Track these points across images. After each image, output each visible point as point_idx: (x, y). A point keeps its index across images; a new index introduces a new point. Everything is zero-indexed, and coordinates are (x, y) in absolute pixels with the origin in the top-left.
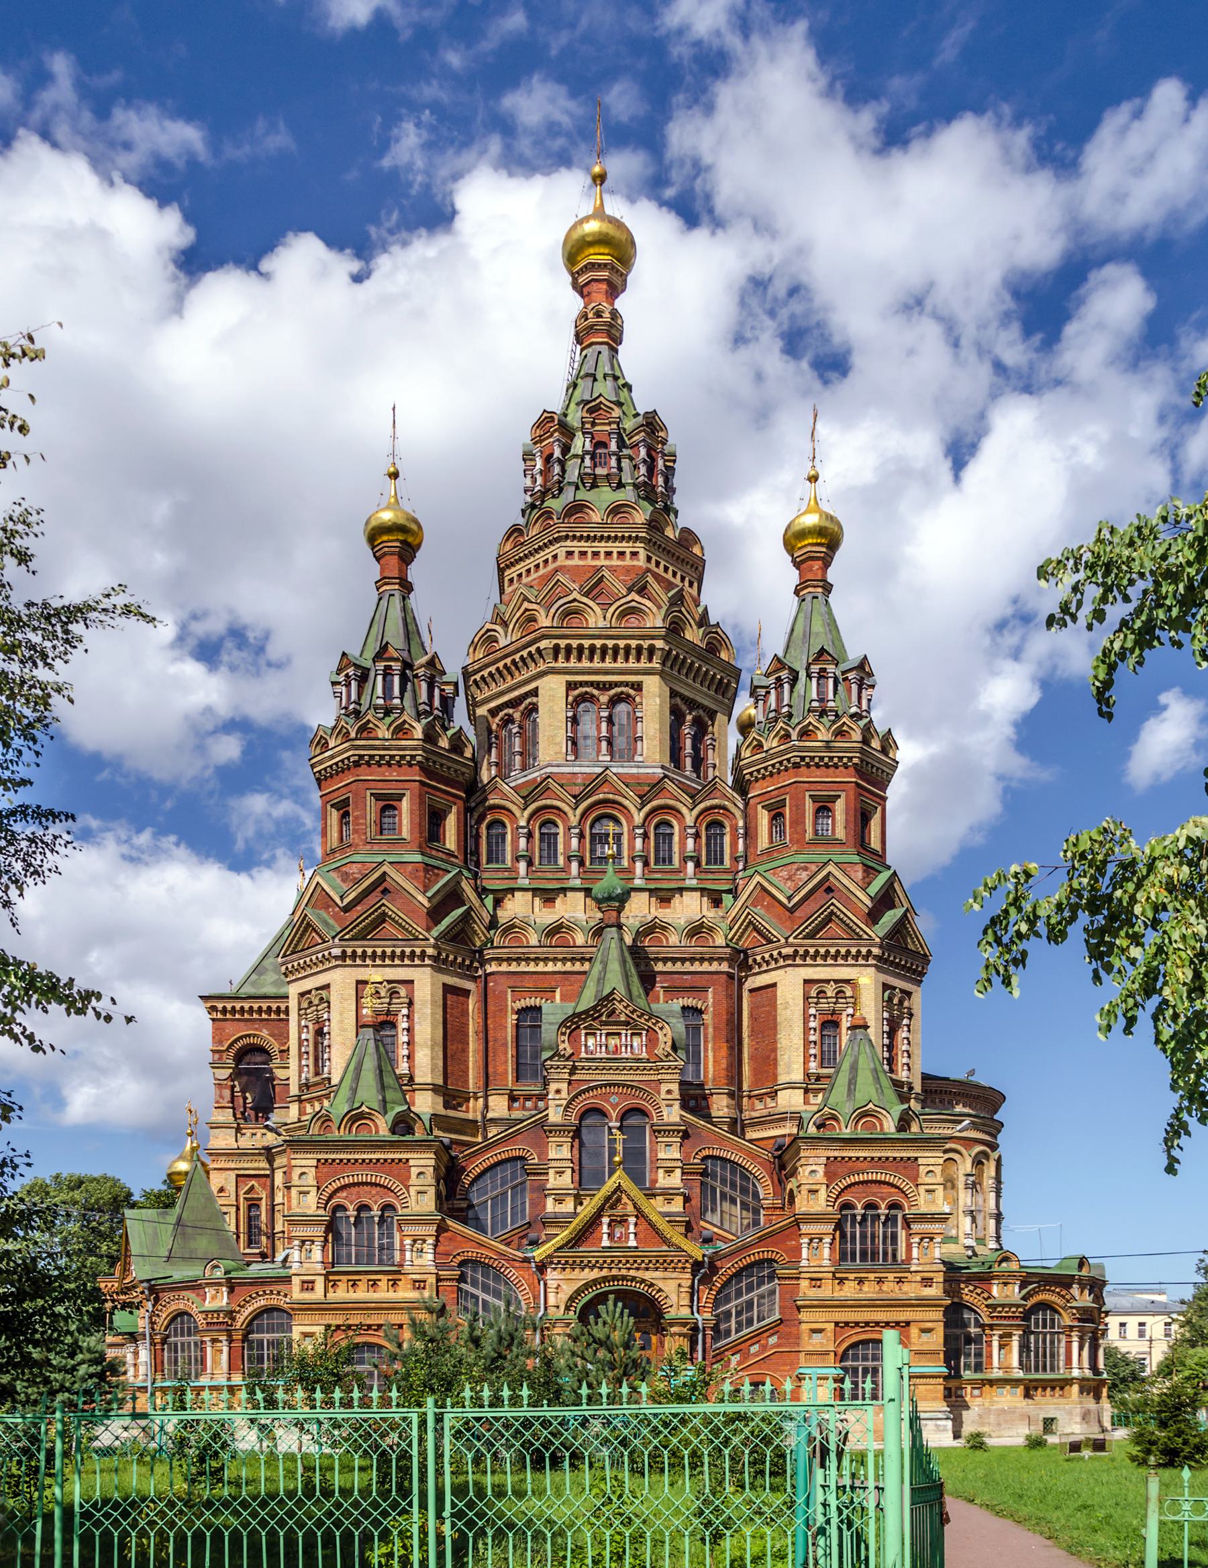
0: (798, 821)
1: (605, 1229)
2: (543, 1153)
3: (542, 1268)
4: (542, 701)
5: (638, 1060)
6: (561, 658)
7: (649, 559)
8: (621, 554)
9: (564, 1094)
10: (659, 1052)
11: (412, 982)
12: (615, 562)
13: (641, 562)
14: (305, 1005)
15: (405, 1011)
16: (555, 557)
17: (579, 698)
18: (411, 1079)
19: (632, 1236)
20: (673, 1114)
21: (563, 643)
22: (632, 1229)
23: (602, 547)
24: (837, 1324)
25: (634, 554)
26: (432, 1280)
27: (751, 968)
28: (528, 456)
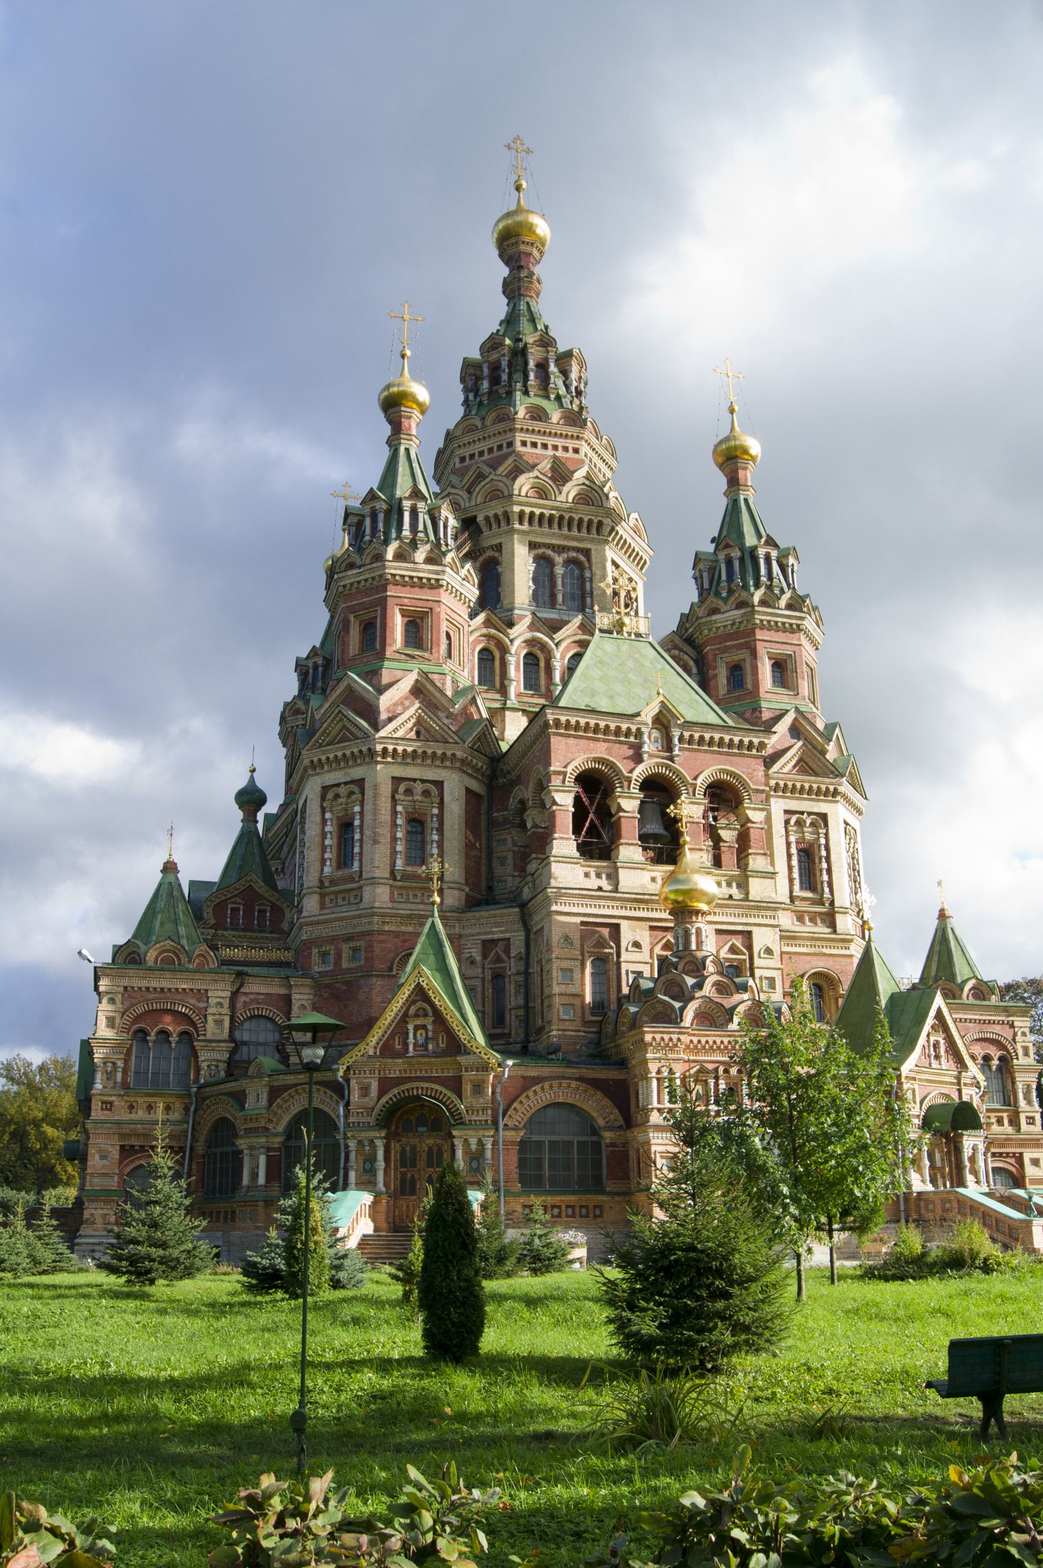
15: (435, 811)
21: (528, 510)
23: (551, 441)
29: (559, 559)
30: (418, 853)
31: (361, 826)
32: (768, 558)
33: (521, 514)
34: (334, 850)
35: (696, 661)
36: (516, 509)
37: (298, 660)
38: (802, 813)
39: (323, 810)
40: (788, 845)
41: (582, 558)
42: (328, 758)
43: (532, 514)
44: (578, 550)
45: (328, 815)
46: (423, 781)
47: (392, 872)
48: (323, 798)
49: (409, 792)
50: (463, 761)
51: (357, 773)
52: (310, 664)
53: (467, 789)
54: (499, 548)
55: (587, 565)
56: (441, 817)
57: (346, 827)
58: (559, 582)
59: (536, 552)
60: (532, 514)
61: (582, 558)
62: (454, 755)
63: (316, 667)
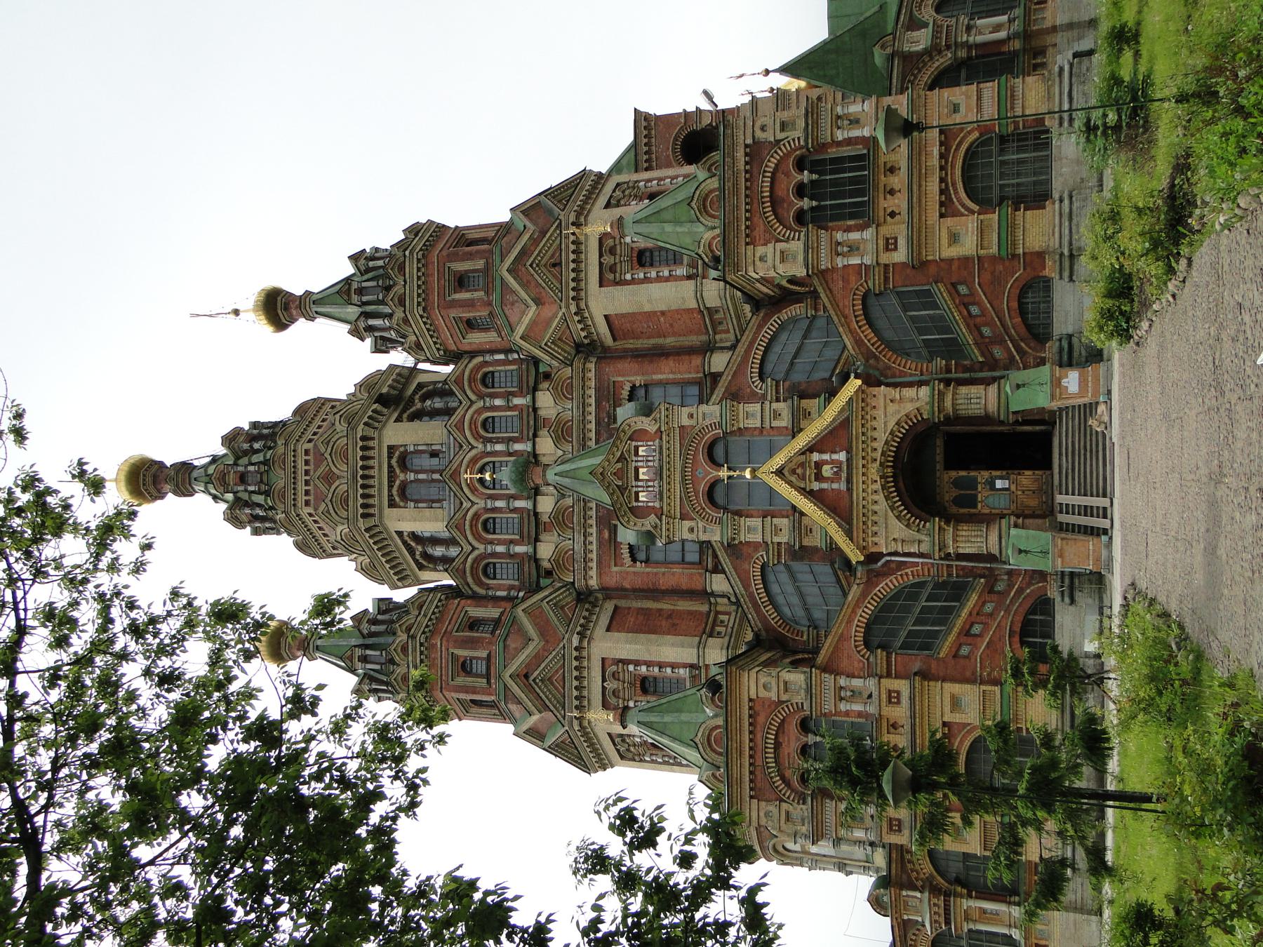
0: (470, 304)
1: (825, 486)
2: (756, 546)
3: (872, 558)
4: (407, 527)
5: (661, 447)
6: (371, 511)
7: (310, 441)
8: (307, 463)
9: (692, 524)
10: (652, 429)
11: (603, 659)
12: (311, 467)
13: (310, 446)
14: (630, 755)
15: (631, 668)
16: (311, 515)
17: (403, 496)
18: (692, 666)
19: (835, 457)
20: (712, 411)
22: (826, 457)
24: (942, 216)
25: (307, 452)
26: (887, 683)
27: (593, 341)
28: (256, 532)
29: (402, 476)
32: (360, 291)
33: (364, 516)
35: (473, 357)
36: (362, 524)
38: (601, 264)
40: (633, 281)
41: (397, 454)
43: (364, 506)
44: (390, 458)
46: (604, 680)
49: (615, 693)
50: (582, 635)
53: (608, 630)
54: (400, 534)
55: (402, 449)
56: (637, 663)
59: (397, 499)
60: (364, 506)
61: (397, 454)
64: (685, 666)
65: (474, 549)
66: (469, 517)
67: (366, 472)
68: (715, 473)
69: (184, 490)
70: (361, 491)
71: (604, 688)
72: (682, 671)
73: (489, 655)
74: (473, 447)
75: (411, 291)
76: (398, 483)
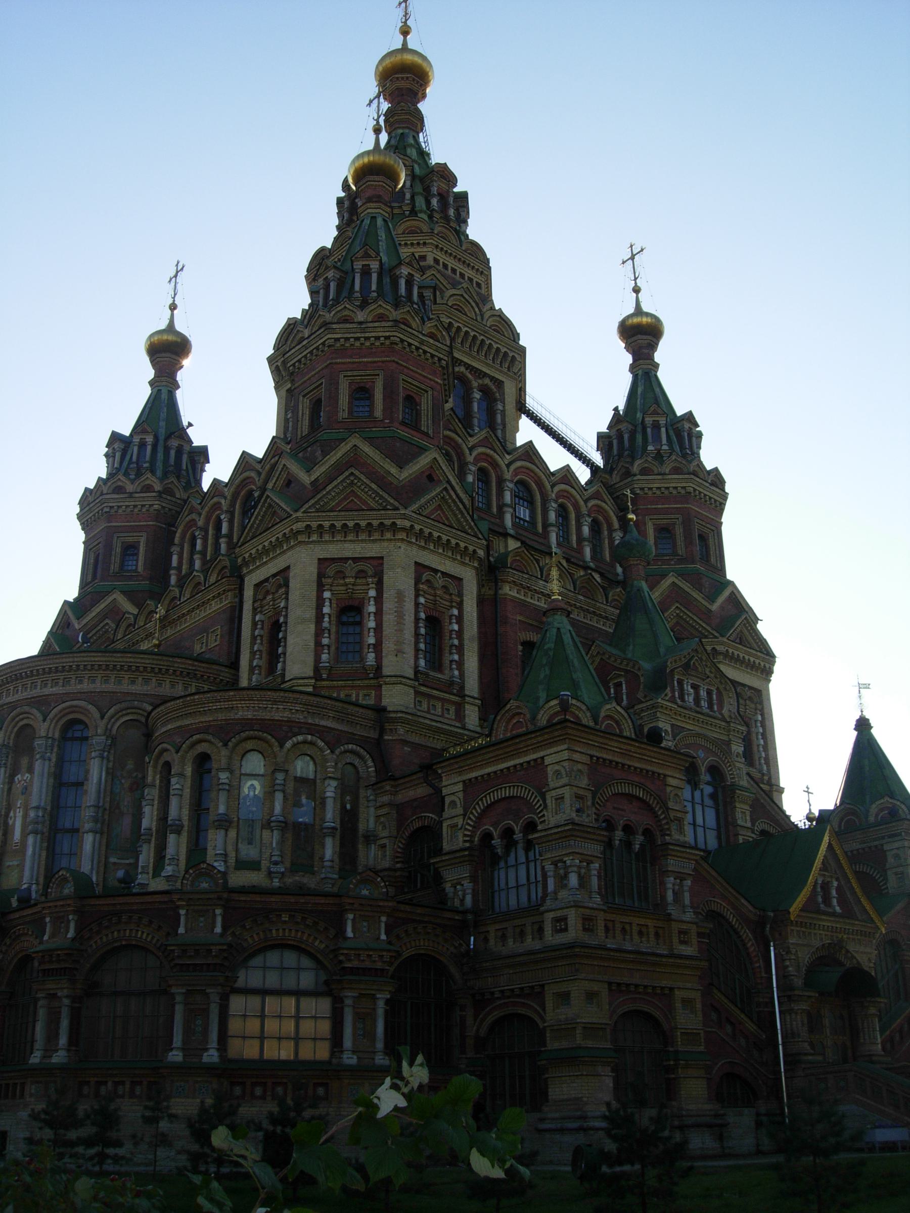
10: (725, 711)
18: (462, 688)
30: (435, 659)
31: (379, 614)
34: (333, 637)
37: (115, 437)
39: (320, 587)
42: (333, 526)
44: (492, 379)
45: (327, 595)
47: (417, 672)
48: (321, 576)
51: (372, 550)
52: (136, 440)
56: (460, 619)
57: (350, 612)
58: (475, 405)
62: (474, 551)
63: (142, 445)
64: (462, 675)
65: (471, 450)
66: (497, 457)
67: (485, 348)
68: (703, 769)
69: (416, 122)
70: (472, 334)
71: (436, 571)
72: (456, 673)
73: (426, 434)
74: (553, 486)
75: (700, 485)
76: (470, 376)
